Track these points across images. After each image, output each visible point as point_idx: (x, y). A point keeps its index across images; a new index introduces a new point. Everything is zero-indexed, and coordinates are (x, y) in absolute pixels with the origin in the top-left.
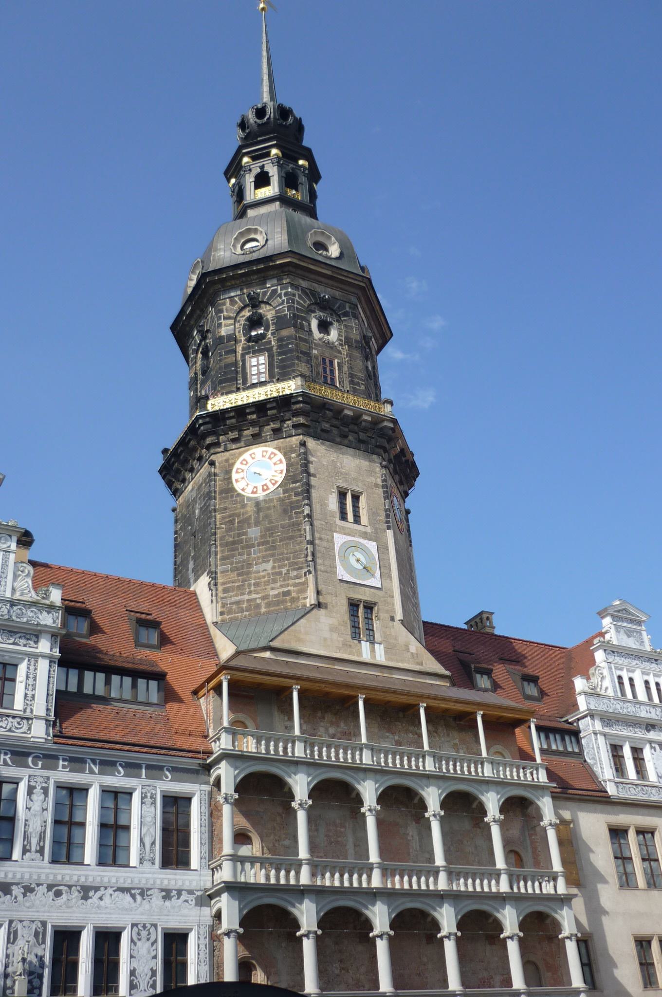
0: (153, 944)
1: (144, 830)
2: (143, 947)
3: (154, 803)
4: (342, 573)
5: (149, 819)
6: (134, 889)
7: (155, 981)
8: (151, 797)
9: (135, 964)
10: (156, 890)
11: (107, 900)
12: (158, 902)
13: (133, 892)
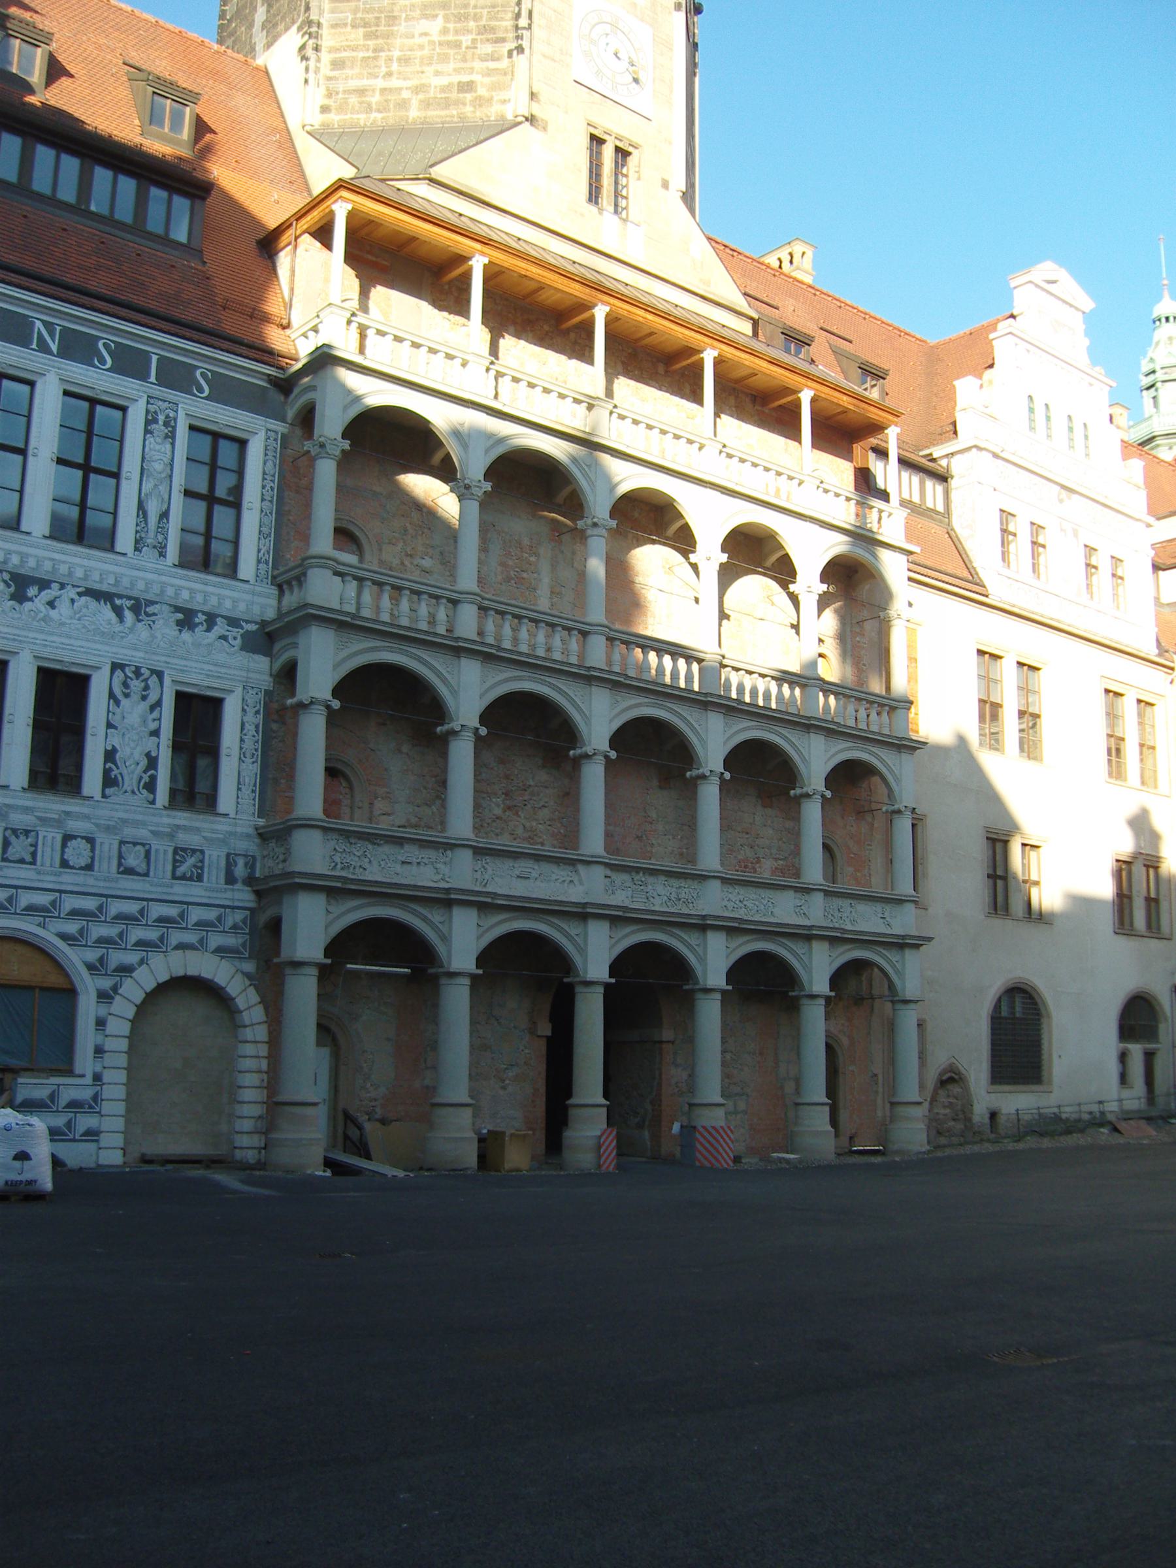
0: (152, 708)
1: (147, 486)
2: (133, 711)
3: (171, 436)
5: (158, 466)
6: (120, 597)
7: (153, 779)
8: (166, 424)
9: (115, 740)
10: (165, 608)
11: (64, 610)
12: (167, 631)
13: (118, 602)
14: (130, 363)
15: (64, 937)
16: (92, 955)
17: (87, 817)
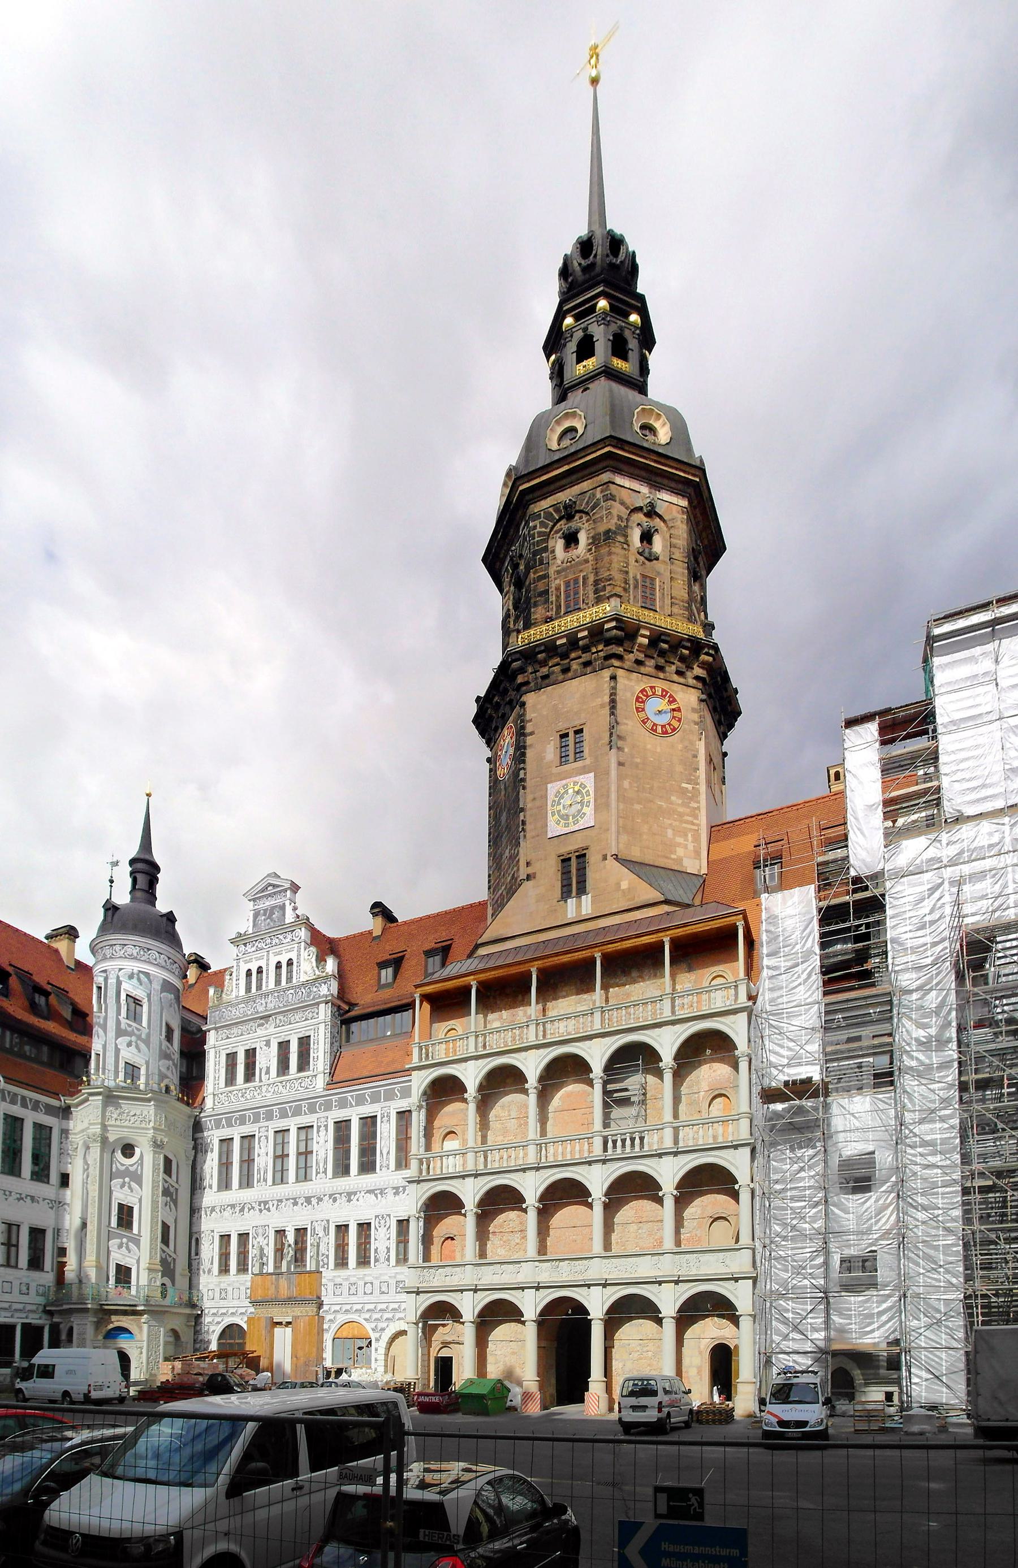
2: (382, 1231)
4: (555, 828)
9: (377, 1245)
14: (375, 1099)
15: (366, 1319)
16: (373, 1325)
17: (370, 1275)
